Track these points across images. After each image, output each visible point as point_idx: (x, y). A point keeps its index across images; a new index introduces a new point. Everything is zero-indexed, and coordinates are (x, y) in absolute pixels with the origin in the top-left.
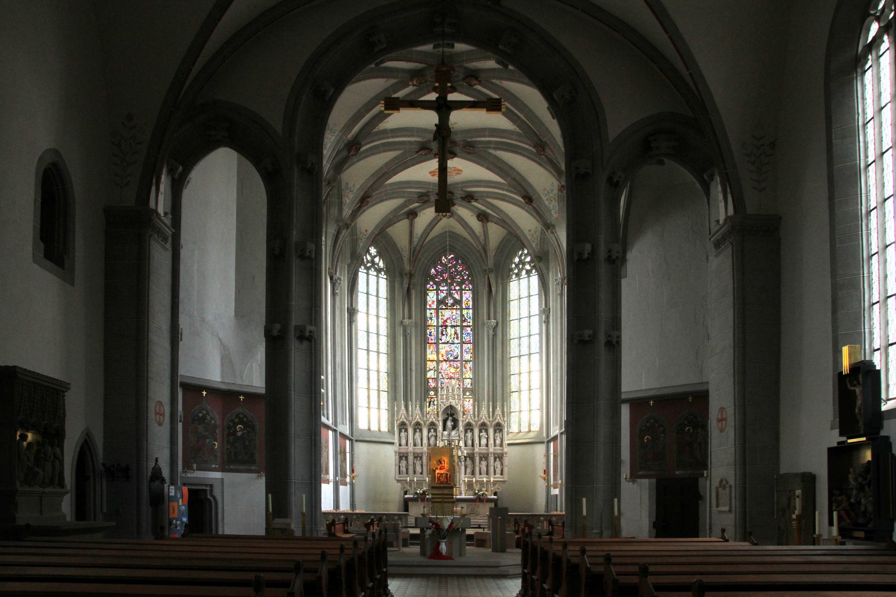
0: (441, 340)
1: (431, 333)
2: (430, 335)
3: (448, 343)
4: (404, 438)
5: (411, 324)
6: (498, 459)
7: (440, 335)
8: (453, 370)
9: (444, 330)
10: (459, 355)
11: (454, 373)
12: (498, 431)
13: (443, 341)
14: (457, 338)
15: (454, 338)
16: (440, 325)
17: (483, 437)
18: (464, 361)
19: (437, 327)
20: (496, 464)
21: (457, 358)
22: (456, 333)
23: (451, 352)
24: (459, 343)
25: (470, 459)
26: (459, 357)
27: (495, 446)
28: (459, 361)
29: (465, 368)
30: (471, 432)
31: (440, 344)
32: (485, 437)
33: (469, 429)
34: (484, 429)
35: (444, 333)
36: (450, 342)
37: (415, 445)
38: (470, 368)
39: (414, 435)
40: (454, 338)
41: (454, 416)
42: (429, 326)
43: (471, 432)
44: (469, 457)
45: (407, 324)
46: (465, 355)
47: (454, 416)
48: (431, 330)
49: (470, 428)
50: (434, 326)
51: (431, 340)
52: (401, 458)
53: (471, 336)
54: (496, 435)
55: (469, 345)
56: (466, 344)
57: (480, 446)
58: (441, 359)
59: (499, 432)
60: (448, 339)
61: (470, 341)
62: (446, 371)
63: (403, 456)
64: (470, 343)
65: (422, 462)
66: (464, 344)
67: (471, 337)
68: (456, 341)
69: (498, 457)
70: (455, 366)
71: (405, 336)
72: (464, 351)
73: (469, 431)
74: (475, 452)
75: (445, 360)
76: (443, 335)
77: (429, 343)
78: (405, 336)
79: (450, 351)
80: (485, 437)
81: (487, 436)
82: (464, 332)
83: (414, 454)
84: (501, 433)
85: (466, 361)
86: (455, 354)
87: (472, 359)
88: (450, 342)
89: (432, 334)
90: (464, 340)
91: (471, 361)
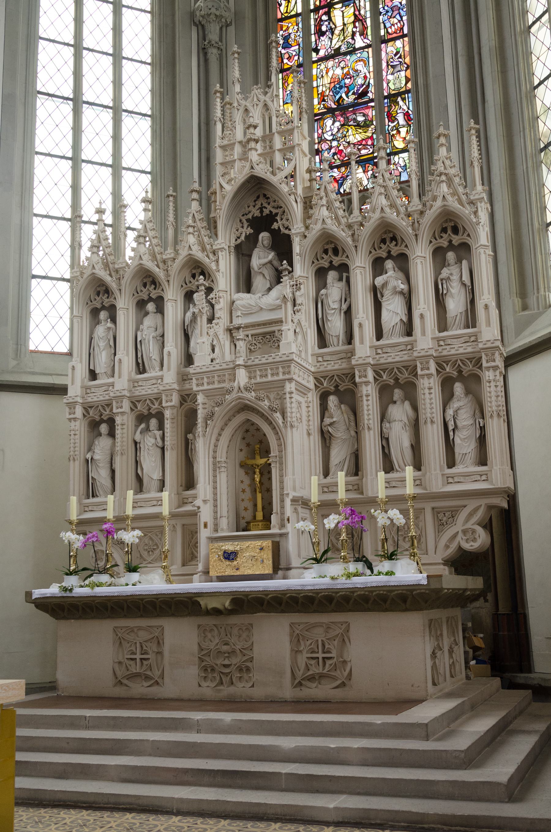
0: (317, 51)
1: (286, 38)
2: (287, 45)
3: (337, 53)
4: (102, 344)
5: (213, 10)
6: (458, 388)
7: (313, 38)
8: (354, 136)
9: (325, 18)
10: (372, 82)
11: (360, 143)
12: (451, 256)
13: (322, 53)
14: (363, 34)
15: (354, 34)
16: (312, 7)
17: (387, 293)
18: (386, 97)
19: (305, 15)
20: (450, 412)
21: (365, 93)
22: (358, 18)
23: (347, 81)
24: (368, 46)
25: (341, 402)
26: (372, 89)
27: (443, 325)
28: (372, 100)
29: (392, 118)
30: (340, 279)
31: (315, 65)
32: (396, 292)
33: (332, 267)
34: (389, 256)
35: (324, 28)
36: (343, 49)
37: (141, 368)
38: (407, 115)
39: (137, 329)
40: (354, 34)
41: (275, 226)
42: (282, 20)
43: (340, 279)
44: (337, 392)
45: (202, 13)
46: (390, 77)
47: (275, 226)
48: (288, 28)
49: (337, 261)
50: (297, 15)
51: (289, 58)
52: (94, 425)
53: (402, 13)
54: (445, 272)
55: (399, 43)
56: (390, 44)
57: (379, 335)
58: (318, 107)
59: (459, 261)
60: (336, 43)
61: (402, 29)
62: (335, 144)
63: (102, 421)
64: (404, 36)
65: (163, 438)
66: (383, 45)
67: (405, 18)
68: (359, 42)
69: (461, 377)
70: (360, 119)
71: (205, 54)
72: (384, 65)
73: (332, 275)
74: (354, 362)
75: (330, 111)
76: (320, 33)
77: (282, 71)
78: (203, 52)
79: (346, 76)
80: (396, 292)
81: (403, 287)
82: (381, 6)
83: (134, 405)
84: (464, 262)
85: (393, 98)
86: (360, 81)
87: (409, 85)
88: (343, 49)
89: (291, 41)
90: (382, 32)
91: (408, 92)
